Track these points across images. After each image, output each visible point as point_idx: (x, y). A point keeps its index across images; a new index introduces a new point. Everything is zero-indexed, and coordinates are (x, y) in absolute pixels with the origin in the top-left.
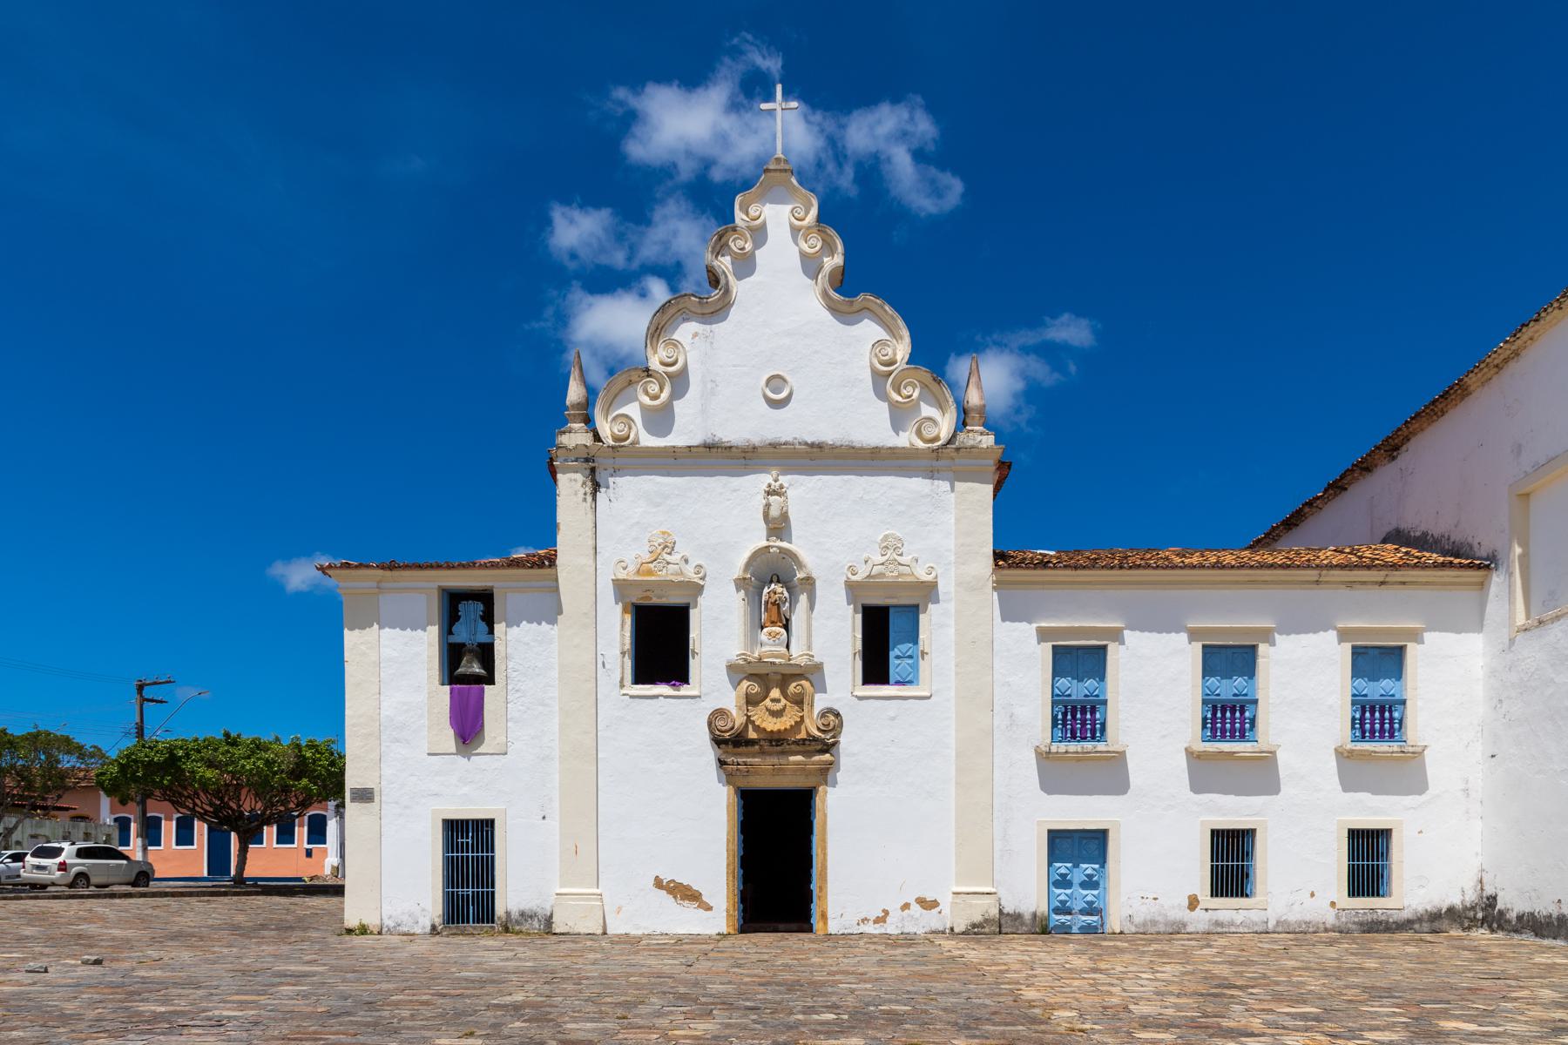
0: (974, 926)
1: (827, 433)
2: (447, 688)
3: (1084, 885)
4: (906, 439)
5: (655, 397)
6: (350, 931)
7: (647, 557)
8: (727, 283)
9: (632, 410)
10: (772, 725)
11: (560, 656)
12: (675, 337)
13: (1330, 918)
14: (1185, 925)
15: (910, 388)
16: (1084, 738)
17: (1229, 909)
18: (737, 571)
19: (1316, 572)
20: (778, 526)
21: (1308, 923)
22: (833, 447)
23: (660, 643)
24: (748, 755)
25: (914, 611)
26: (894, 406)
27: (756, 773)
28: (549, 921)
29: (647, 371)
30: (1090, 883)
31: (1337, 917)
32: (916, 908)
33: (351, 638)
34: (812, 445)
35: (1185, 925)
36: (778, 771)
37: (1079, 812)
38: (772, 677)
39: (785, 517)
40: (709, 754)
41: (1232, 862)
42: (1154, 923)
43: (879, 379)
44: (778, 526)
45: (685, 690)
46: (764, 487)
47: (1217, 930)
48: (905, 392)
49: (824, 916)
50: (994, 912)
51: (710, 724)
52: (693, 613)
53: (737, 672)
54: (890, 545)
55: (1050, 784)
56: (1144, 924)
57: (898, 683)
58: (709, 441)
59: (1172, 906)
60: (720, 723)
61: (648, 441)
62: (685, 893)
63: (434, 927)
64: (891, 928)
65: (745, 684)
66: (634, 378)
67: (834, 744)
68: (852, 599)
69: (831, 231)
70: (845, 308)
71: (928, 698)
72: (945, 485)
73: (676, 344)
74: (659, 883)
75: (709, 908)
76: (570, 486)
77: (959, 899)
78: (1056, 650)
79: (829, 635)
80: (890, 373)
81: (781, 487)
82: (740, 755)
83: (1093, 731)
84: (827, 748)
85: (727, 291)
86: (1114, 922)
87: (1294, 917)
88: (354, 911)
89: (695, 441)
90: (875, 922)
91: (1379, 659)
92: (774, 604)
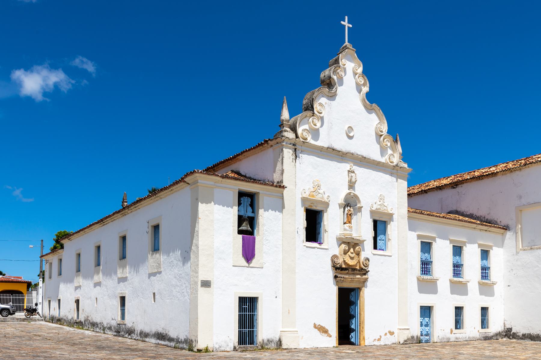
0: (405, 341)
2: (241, 236)
4: (383, 160)
6: (199, 351)
7: (312, 190)
9: (306, 127)
10: (351, 263)
11: (279, 226)
19: (475, 225)
20: (352, 185)
25: (385, 223)
26: (381, 148)
28: (279, 343)
30: (427, 325)
32: (388, 334)
33: (202, 207)
36: (352, 281)
37: (427, 300)
40: (330, 273)
42: (444, 338)
43: (379, 136)
44: (352, 185)
45: (323, 246)
46: (348, 169)
49: (364, 338)
52: (325, 214)
53: (341, 241)
54: (382, 198)
55: (421, 290)
57: (380, 249)
58: (330, 147)
60: (335, 260)
62: (323, 330)
63: (235, 348)
64: (382, 343)
65: (343, 246)
66: (308, 115)
68: (372, 216)
69: (366, 78)
70: (369, 107)
71: (391, 256)
72: (395, 179)
73: (321, 104)
74: (315, 326)
75: (331, 336)
76: (288, 153)
78: (422, 243)
79: (363, 229)
89: (326, 145)
90: (378, 340)
91: (485, 254)
92: (350, 215)
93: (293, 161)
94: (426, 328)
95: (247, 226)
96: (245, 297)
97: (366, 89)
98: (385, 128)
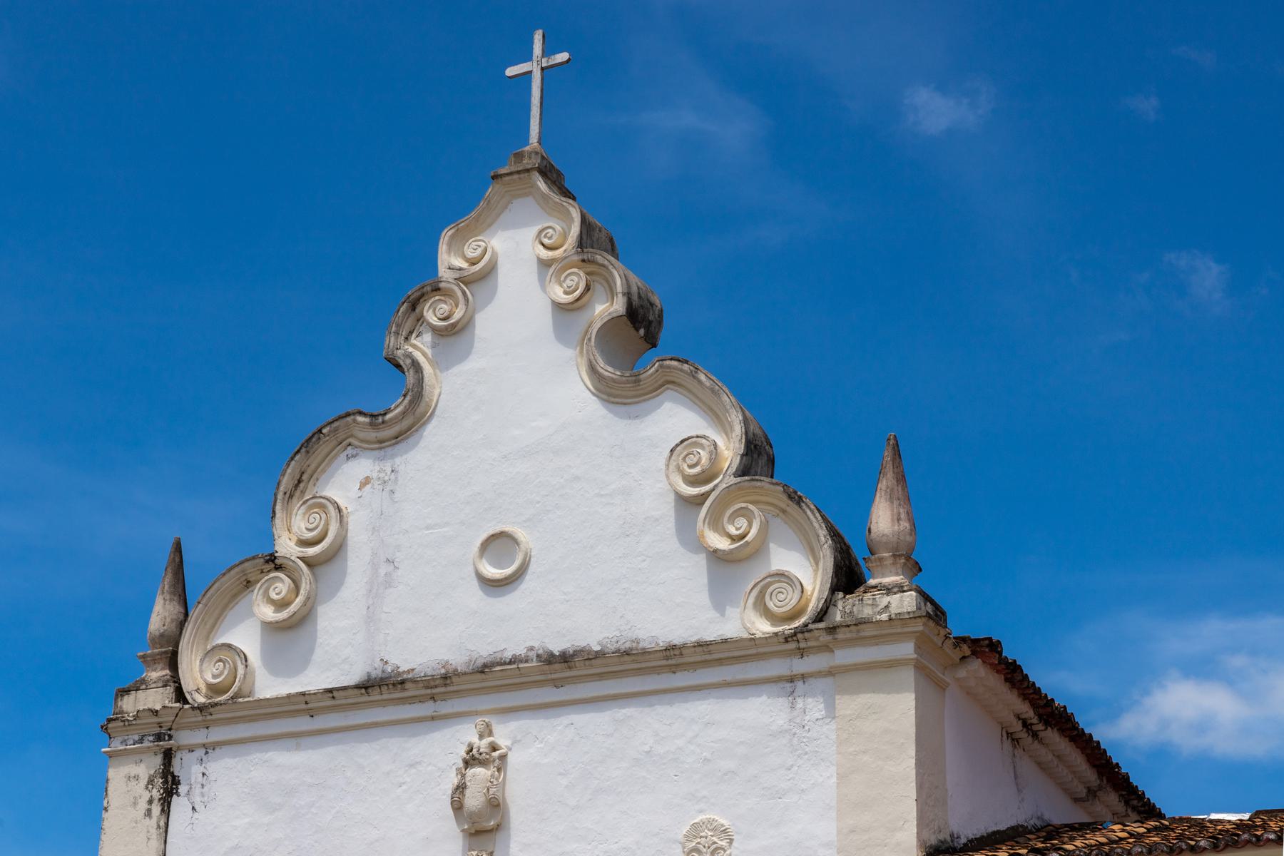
1: (592, 632)
5: (281, 605)
8: (420, 381)
12: (324, 494)
15: (742, 523)
22: (599, 655)
29: (273, 562)
34: (550, 659)
39: (495, 805)
46: (462, 752)
48: (732, 530)
61: (269, 687)
72: (813, 707)
80: (705, 496)
81: (494, 748)
85: (417, 394)
93: (148, 813)
97: (606, 308)
98: (730, 450)
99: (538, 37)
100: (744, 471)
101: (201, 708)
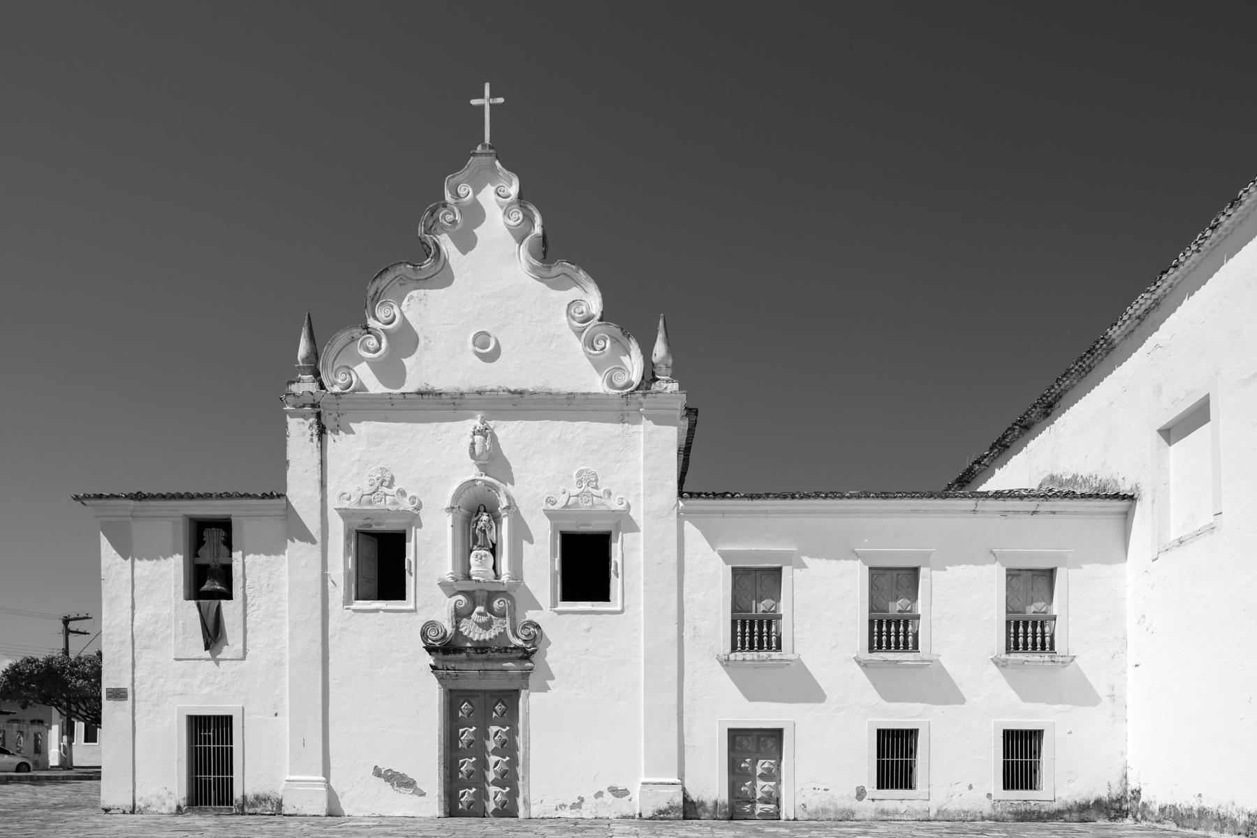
2: (193, 603)
3: (762, 777)
4: (598, 385)
7: (367, 490)
13: (987, 809)
14: (853, 813)
16: (761, 648)
17: (894, 799)
18: (448, 503)
21: (966, 812)
23: (383, 563)
24: (455, 661)
27: (465, 677)
31: (993, 807)
32: (608, 797)
34: (515, 392)
35: (853, 813)
38: (477, 594)
41: (896, 756)
42: (825, 811)
47: (884, 817)
50: (679, 800)
51: (424, 635)
56: (816, 813)
59: (843, 798)
61: (375, 387)
67: (533, 652)
69: (532, 208)
77: (647, 789)
78: (735, 571)
82: (450, 661)
83: (769, 643)
84: (526, 655)
86: (787, 810)
87: (953, 806)
88: (112, 792)
94: (763, 783)
95: (210, 582)
96: (205, 717)
99: (487, 86)
100: (601, 320)
101: (336, 394)
